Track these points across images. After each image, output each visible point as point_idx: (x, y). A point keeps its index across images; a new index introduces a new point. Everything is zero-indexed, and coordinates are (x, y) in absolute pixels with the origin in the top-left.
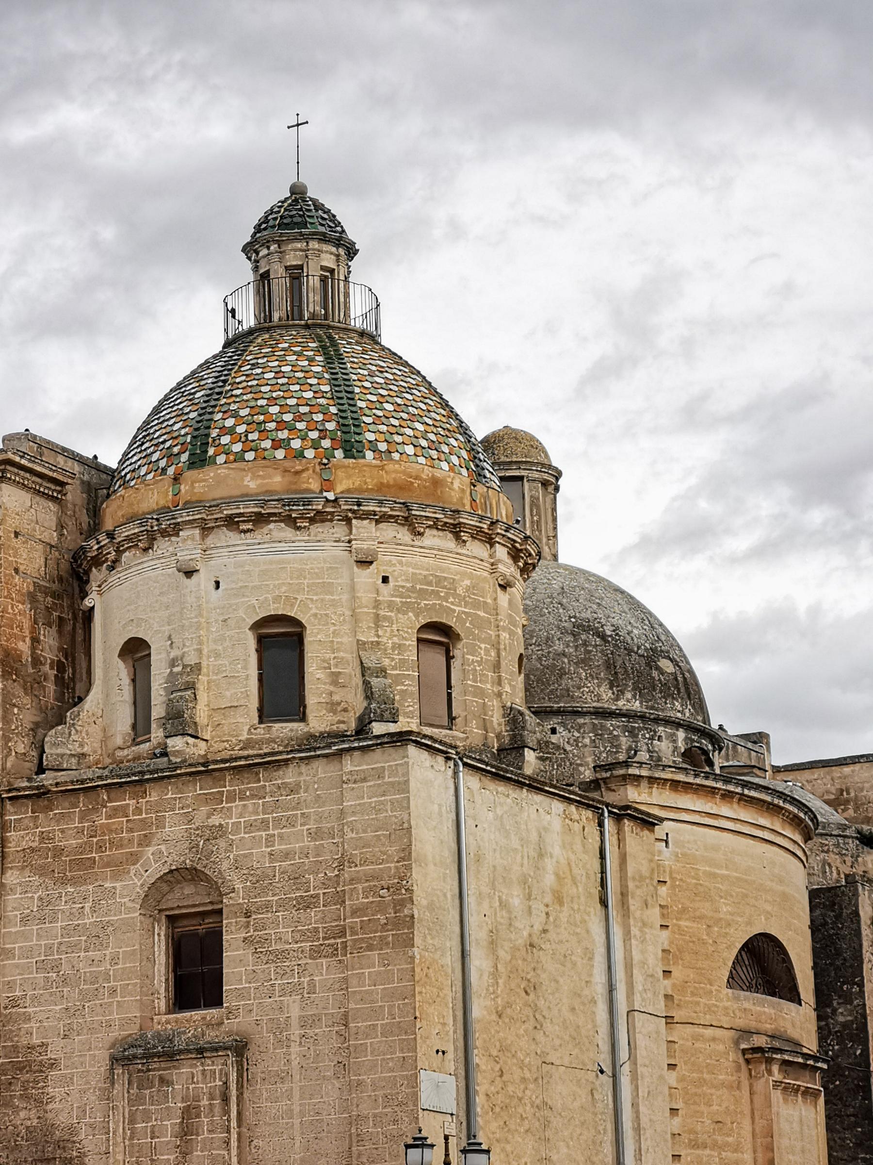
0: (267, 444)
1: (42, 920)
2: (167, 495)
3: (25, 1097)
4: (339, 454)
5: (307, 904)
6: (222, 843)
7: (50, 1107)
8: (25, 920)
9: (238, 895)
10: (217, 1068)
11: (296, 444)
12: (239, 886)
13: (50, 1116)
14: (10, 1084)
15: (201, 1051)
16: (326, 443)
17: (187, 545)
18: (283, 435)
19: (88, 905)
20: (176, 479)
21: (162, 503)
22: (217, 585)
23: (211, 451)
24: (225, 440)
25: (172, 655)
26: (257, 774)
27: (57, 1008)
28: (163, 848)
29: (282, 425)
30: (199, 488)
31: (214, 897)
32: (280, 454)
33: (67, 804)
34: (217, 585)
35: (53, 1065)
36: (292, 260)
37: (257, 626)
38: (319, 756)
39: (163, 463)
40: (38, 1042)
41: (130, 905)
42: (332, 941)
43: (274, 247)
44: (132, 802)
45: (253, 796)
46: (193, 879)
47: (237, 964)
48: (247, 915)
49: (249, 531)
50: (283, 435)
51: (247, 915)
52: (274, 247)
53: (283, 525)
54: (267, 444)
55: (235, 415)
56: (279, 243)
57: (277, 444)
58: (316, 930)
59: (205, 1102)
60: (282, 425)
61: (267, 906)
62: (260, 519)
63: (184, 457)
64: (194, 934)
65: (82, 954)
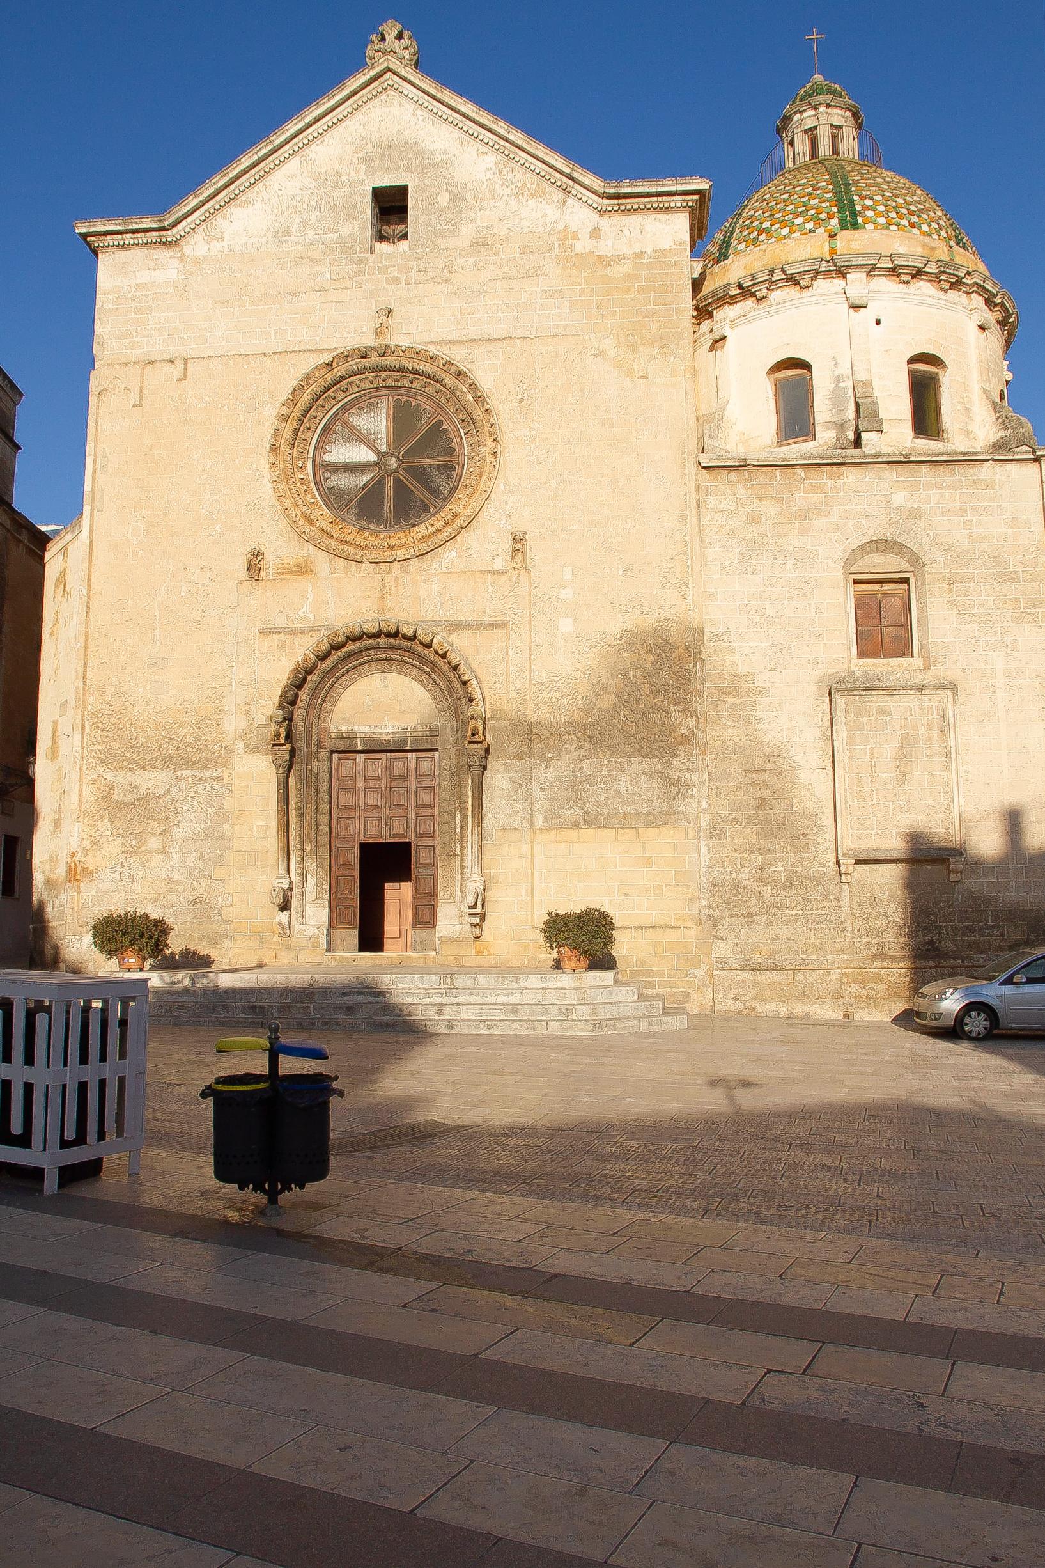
0: (904, 222)
1: (744, 571)
2: (822, 247)
3: (732, 715)
4: (952, 243)
5: (1007, 578)
6: (922, 523)
7: (759, 727)
8: (726, 570)
9: (938, 565)
10: (935, 705)
11: (925, 228)
12: (940, 558)
13: (759, 734)
14: (717, 705)
15: (921, 688)
16: (943, 233)
17: (856, 282)
18: (914, 219)
19: (790, 563)
20: (832, 236)
21: (816, 254)
22: (878, 322)
23: (860, 220)
24: (870, 213)
25: (838, 372)
26: (953, 470)
27: (763, 645)
28: (863, 521)
29: (911, 213)
30: (855, 246)
31: (906, 567)
32: (916, 231)
33: (763, 477)
34: (878, 322)
35: (761, 691)
36: (836, 121)
37: (911, 361)
38: (1012, 460)
39: (810, 225)
40: (744, 672)
41: (833, 565)
42: (1033, 610)
43: (822, 109)
44: (831, 482)
45: (949, 487)
46: (884, 551)
47: (937, 620)
48: (950, 582)
49: (908, 283)
50: (914, 219)
51: (950, 582)
52: (822, 109)
53: (929, 284)
54: (904, 222)
55: (872, 199)
56: (828, 106)
57: (912, 225)
58: (1017, 600)
59: (923, 731)
60: (911, 213)
61: (969, 578)
62: (918, 274)
63: (834, 222)
64: (873, 596)
65: (786, 602)
